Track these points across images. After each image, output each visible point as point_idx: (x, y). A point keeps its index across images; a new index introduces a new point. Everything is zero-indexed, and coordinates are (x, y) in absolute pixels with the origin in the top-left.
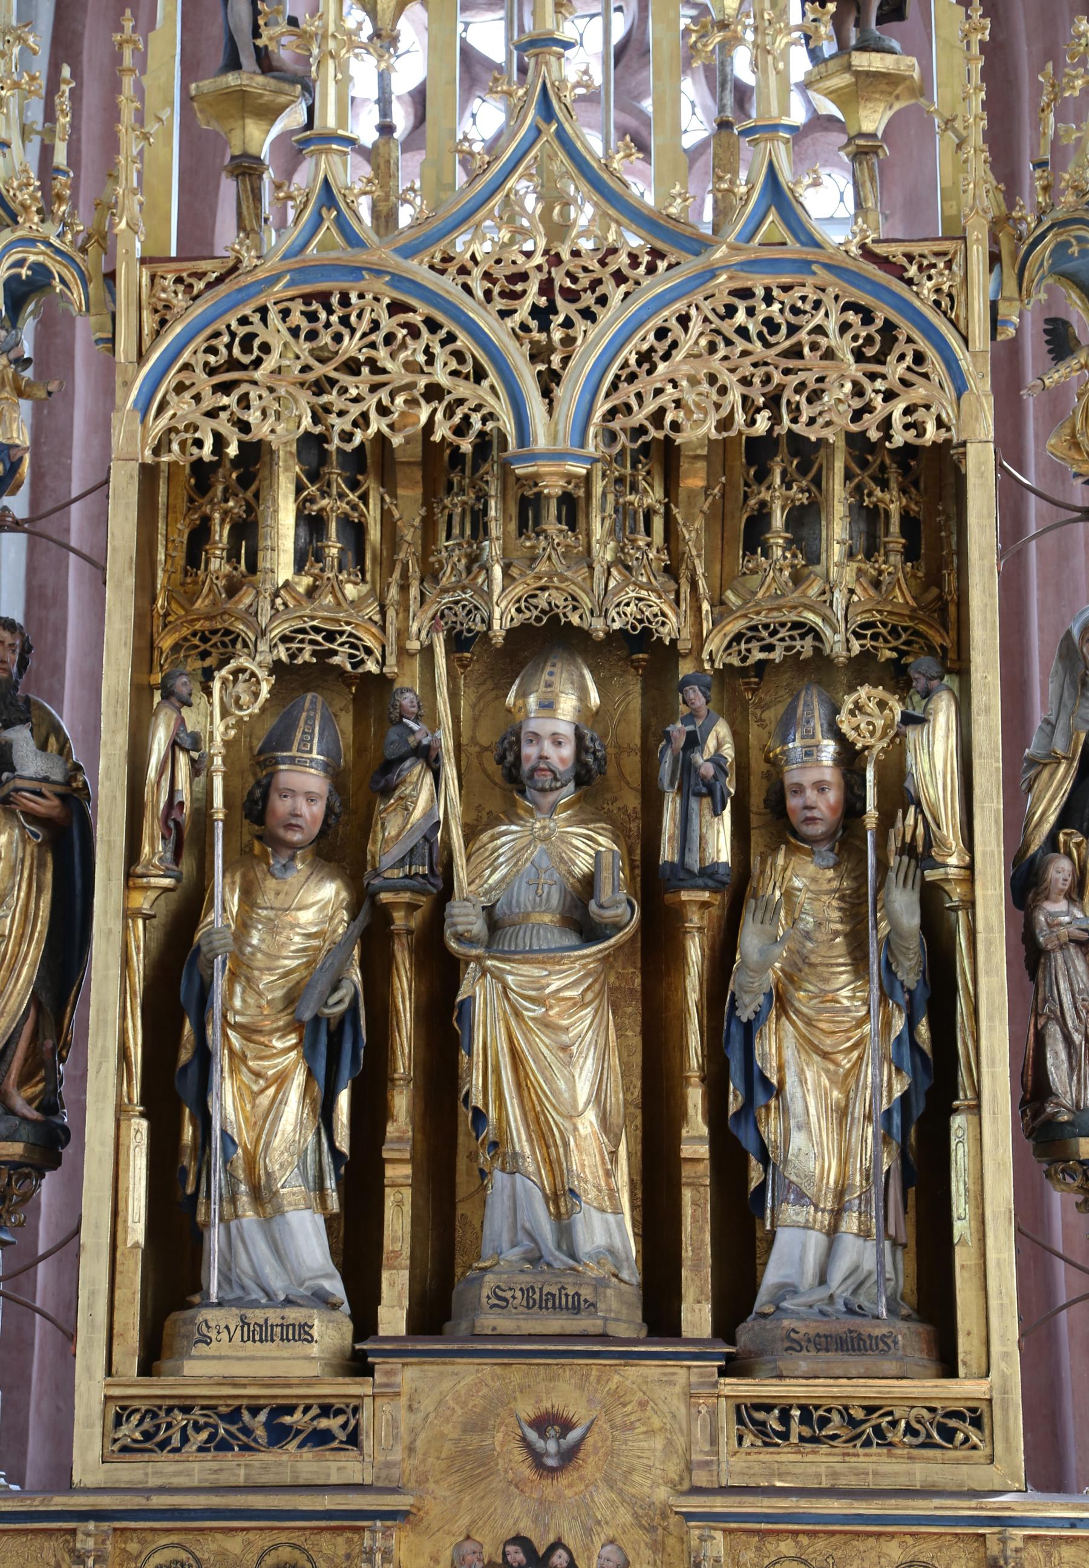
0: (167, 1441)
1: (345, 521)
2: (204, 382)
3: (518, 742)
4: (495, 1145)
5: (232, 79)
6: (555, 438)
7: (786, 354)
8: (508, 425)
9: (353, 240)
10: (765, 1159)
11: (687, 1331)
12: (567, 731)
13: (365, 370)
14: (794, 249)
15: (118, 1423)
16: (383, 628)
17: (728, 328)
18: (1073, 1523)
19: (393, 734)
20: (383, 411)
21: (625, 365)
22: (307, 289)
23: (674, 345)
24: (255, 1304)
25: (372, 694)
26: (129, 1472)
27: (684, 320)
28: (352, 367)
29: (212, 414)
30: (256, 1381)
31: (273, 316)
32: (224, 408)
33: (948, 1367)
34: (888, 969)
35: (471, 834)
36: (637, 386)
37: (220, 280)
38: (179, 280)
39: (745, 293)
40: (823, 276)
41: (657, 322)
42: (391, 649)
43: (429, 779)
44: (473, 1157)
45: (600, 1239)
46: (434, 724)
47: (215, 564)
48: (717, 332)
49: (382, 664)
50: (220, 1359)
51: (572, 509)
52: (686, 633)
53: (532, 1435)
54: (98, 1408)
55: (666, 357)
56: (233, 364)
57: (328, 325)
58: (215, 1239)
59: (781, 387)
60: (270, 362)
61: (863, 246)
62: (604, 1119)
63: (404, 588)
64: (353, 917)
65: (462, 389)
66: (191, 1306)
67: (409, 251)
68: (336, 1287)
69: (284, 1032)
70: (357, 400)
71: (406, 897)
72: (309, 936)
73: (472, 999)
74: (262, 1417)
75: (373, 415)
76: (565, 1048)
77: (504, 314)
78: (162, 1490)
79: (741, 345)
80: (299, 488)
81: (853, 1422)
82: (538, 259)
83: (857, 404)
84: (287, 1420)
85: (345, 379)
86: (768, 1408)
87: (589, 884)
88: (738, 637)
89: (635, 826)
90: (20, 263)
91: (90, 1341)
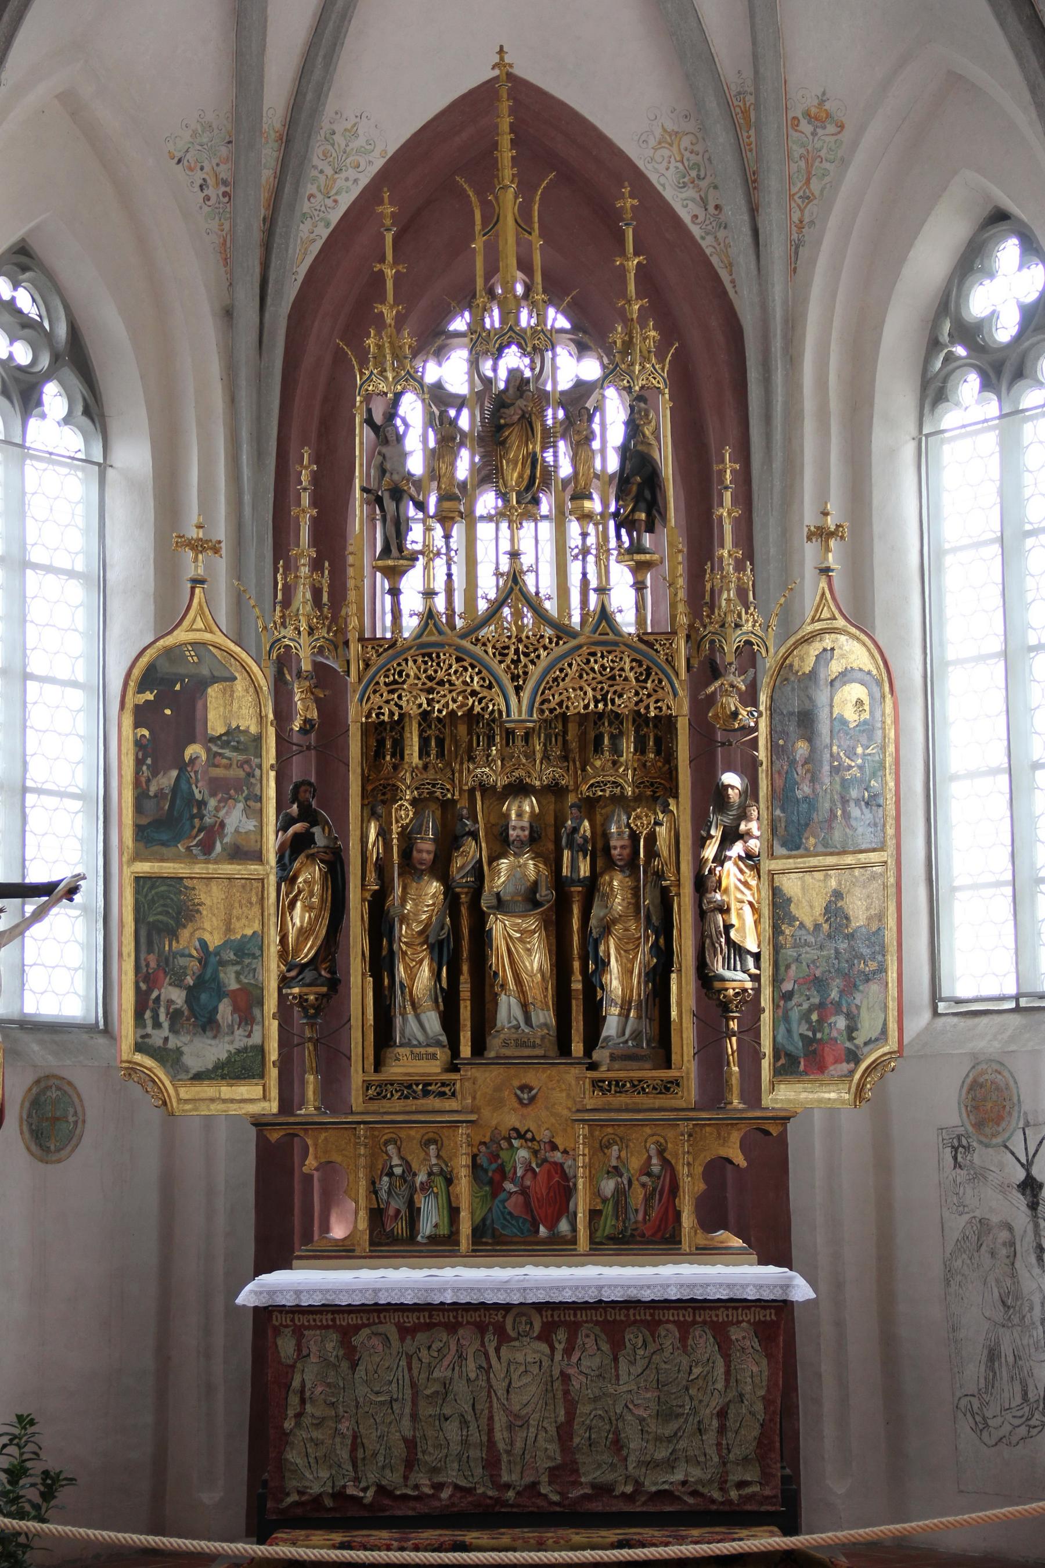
0: (385, 1097)
1: (437, 738)
2: (384, 689)
4: (502, 986)
5: (390, 563)
6: (520, 714)
7: (609, 679)
8: (504, 709)
9: (440, 632)
10: (602, 988)
11: (574, 1054)
12: (526, 824)
13: (447, 685)
14: (611, 636)
15: (367, 1090)
16: (453, 780)
18: (710, 1119)
19: (459, 827)
20: (454, 701)
21: (548, 683)
23: (566, 675)
24: (415, 1046)
25: (447, 805)
26: (374, 1106)
27: (570, 665)
28: (441, 683)
29: (387, 702)
30: (417, 1074)
31: (410, 663)
32: (393, 699)
33: (669, 1066)
34: (648, 917)
35: (490, 863)
38: (373, 648)
39: (594, 654)
40: (623, 648)
41: (560, 666)
43: (474, 843)
44: (492, 986)
45: (542, 1020)
46: (476, 821)
47: (388, 758)
48: (582, 669)
49: (453, 795)
50: (403, 1065)
51: (527, 737)
52: (572, 783)
53: (519, 1092)
54: (360, 1084)
55: (563, 680)
56: (395, 682)
57: (432, 666)
58: (398, 1021)
59: (608, 692)
60: (411, 681)
61: (638, 636)
62: (543, 975)
63: (462, 763)
64: (445, 899)
65: (485, 693)
66: (391, 1046)
67: (463, 636)
68: (444, 1039)
69: (422, 944)
70: (445, 696)
71: (466, 890)
72: (428, 906)
73: (491, 929)
74: (420, 1087)
75: (450, 702)
76: (529, 950)
77: (501, 662)
78: (385, 1113)
79: (592, 675)
80: (420, 725)
81: (634, 1086)
82: (514, 640)
84: (430, 1088)
85: (439, 688)
86: (604, 1081)
87: (536, 883)
88: (592, 785)
89: (552, 856)
90: (314, 647)
91: (356, 1061)
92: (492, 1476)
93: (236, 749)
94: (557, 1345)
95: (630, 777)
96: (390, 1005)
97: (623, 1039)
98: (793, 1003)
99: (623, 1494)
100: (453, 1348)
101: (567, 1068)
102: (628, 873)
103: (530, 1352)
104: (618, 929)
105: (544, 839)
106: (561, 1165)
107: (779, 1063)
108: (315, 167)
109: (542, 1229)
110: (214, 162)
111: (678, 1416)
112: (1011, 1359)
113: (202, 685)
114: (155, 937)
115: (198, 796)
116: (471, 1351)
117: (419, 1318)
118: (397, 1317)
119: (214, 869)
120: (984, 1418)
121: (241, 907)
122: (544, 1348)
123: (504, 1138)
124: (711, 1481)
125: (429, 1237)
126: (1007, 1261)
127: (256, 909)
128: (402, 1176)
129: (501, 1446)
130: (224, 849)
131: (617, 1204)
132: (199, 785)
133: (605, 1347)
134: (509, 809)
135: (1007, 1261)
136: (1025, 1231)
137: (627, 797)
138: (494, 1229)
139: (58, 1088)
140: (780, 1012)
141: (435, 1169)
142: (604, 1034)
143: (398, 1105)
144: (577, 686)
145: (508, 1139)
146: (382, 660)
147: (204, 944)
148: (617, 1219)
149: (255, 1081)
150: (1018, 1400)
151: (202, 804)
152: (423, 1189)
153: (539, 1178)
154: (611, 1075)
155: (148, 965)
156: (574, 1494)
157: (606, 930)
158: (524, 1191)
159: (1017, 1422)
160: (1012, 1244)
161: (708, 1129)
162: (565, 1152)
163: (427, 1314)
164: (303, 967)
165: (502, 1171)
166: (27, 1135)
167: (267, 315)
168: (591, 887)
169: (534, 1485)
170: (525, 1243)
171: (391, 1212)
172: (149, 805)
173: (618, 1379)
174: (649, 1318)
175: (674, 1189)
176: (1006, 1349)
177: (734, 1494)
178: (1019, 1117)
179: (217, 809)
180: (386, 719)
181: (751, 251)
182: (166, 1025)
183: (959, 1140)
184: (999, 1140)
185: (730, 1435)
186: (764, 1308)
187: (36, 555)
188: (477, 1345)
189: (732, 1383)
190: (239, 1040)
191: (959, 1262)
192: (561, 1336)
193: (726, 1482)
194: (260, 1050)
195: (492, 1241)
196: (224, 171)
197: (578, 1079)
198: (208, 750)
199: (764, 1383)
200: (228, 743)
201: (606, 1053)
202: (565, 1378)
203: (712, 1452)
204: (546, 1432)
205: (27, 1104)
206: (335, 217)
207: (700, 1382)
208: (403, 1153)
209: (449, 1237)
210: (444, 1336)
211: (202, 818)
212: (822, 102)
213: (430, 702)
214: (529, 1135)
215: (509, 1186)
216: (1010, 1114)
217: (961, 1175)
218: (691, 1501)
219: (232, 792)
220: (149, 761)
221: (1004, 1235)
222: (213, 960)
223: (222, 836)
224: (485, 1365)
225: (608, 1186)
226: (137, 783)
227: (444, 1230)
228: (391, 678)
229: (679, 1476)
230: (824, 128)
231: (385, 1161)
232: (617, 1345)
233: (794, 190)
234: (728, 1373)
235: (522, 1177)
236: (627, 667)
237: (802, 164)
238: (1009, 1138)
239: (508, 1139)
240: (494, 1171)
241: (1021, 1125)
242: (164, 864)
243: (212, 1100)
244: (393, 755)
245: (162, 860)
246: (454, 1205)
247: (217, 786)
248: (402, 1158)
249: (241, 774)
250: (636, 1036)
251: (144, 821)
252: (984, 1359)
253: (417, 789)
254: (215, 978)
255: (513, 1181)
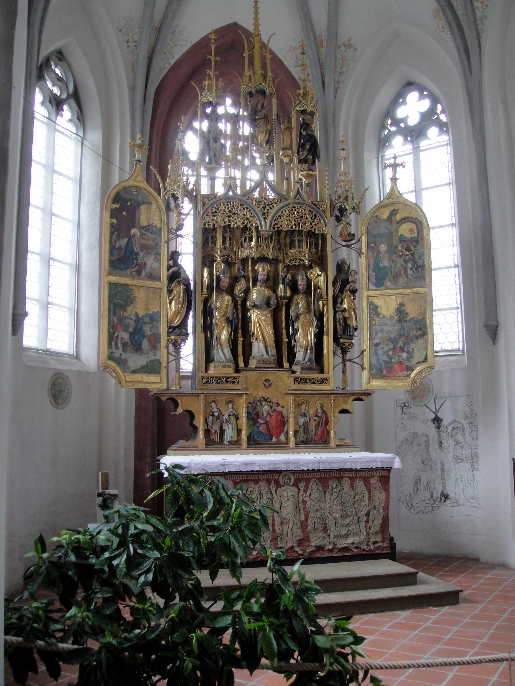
1: (230, 237)
3: (258, 275)
6: (266, 228)
8: (259, 225)
10: (295, 341)
12: (266, 274)
14: (301, 201)
17: (292, 212)
20: (239, 221)
22: (227, 201)
26: (206, 386)
27: (285, 211)
31: (222, 205)
36: (278, 220)
37: (213, 198)
40: (305, 206)
41: (281, 211)
42: (237, 259)
45: (272, 353)
47: (210, 244)
53: (265, 382)
63: (239, 249)
65: (251, 219)
77: (258, 207)
81: (310, 380)
83: (311, 226)
85: (233, 216)
86: (298, 378)
88: (290, 260)
92: (274, 544)
93: (151, 233)
94: (300, 488)
95: (307, 257)
96: (210, 345)
97: (305, 362)
98: (379, 348)
99: (328, 549)
100: (257, 490)
101: (283, 373)
102: (304, 296)
103: (289, 491)
104: (302, 318)
105: (272, 282)
106: (281, 412)
107: (372, 372)
108: (168, 43)
109: (274, 438)
110: (133, 33)
111: (350, 516)
112: (426, 483)
113: (139, 204)
114: (117, 309)
115: (136, 251)
116: (264, 492)
117: (242, 478)
118: (233, 477)
119: (142, 283)
120: (412, 504)
121: (152, 300)
122: (296, 489)
123: (258, 401)
124: (363, 542)
125: (229, 442)
126: (426, 448)
127: (158, 301)
128: (218, 416)
129: (278, 532)
130: (146, 274)
131: (305, 428)
132: (136, 246)
133: (321, 488)
134: (258, 268)
135: (426, 448)
136: (434, 437)
137: (306, 265)
138: (254, 438)
139: (62, 378)
140: (373, 351)
141: (232, 414)
142: (296, 359)
143: (215, 386)
144: (288, 219)
145: (260, 401)
146: (211, 202)
147: (137, 314)
148: (305, 434)
149: (157, 375)
150: (428, 497)
151: (137, 254)
152: (226, 422)
153: (273, 417)
154: (302, 376)
155: (113, 321)
156: (309, 550)
157: (298, 317)
158: (266, 423)
159: (427, 505)
160: (428, 441)
161: (340, 398)
162: (283, 407)
163: (245, 476)
164: (174, 328)
165: (257, 414)
166: (50, 397)
167: (148, 91)
168: (290, 301)
169: (292, 547)
170: (267, 444)
171: (213, 431)
172: (116, 252)
173: (326, 502)
174: (338, 476)
175: (327, 422)
176: (424, 479)
177: (372, 547)
178: (432, 395)
179: (143, 257)
180: (211, 226)
181: (322, 88)
182: (121, 348)
183: (404, 404)
184: (423, 403)
185: (370, 523)
186: (383, 470)
187: (56, 168)
188: (267, 489)
189: (371, 502)
190: (151, 357)
191: (403, 448)
192: (302, 484)
193: (369, 542)
194: (159, 362)
195: (255, 443)
196: (136, 38)
197: (288, 377)
198: (140, 232)
199: (384, 501)
200: (149, 230)
201: (300, 367)
202: (304, 502)
203: (363, 530)
204: (297, 525)
205: (50, 384)
206: (173, 62)
207: (359, 502)
208: (218, 407)
209: (237, 441)
210: (253, 485)
211: (137, 260)
212: (349, 41)
213: (229, 221)
214: (269, 400)
215: (260, 421)
216: (428, 394)
217: (404, 417)
218: (355, 550)
219: (150, 250)
220: (116, 233)
221: (425, 438)
222: (141, 321)
223: (145, 269)
224: (270, 497)
225: (301, 421)
226: (111, 242)
227: (235, 439)
228: (214, 210)
229: (350, 541)
230: (349, 49)
231: (211, 410)
232: (325, 487)
233: (337, 70)
234: (370, 498)
235: (266, 417)
236: (307, 214)
237: (341, 61)
238: (428, 403)
239: (260, 401)
240: (254, 415)
241: (433, 398)
242: (122, 278)
243: (140, 382)
244: (212, 243)
245: (120, 276)
246: (239, 428)
247: (144, 247)
248: (218, 409)
249: (154, 243)
250: (310, 360)
251: (114, 259)
252: (413, 483)
253: (222, 257)
254: (141, 329)
255: (262, 419)
